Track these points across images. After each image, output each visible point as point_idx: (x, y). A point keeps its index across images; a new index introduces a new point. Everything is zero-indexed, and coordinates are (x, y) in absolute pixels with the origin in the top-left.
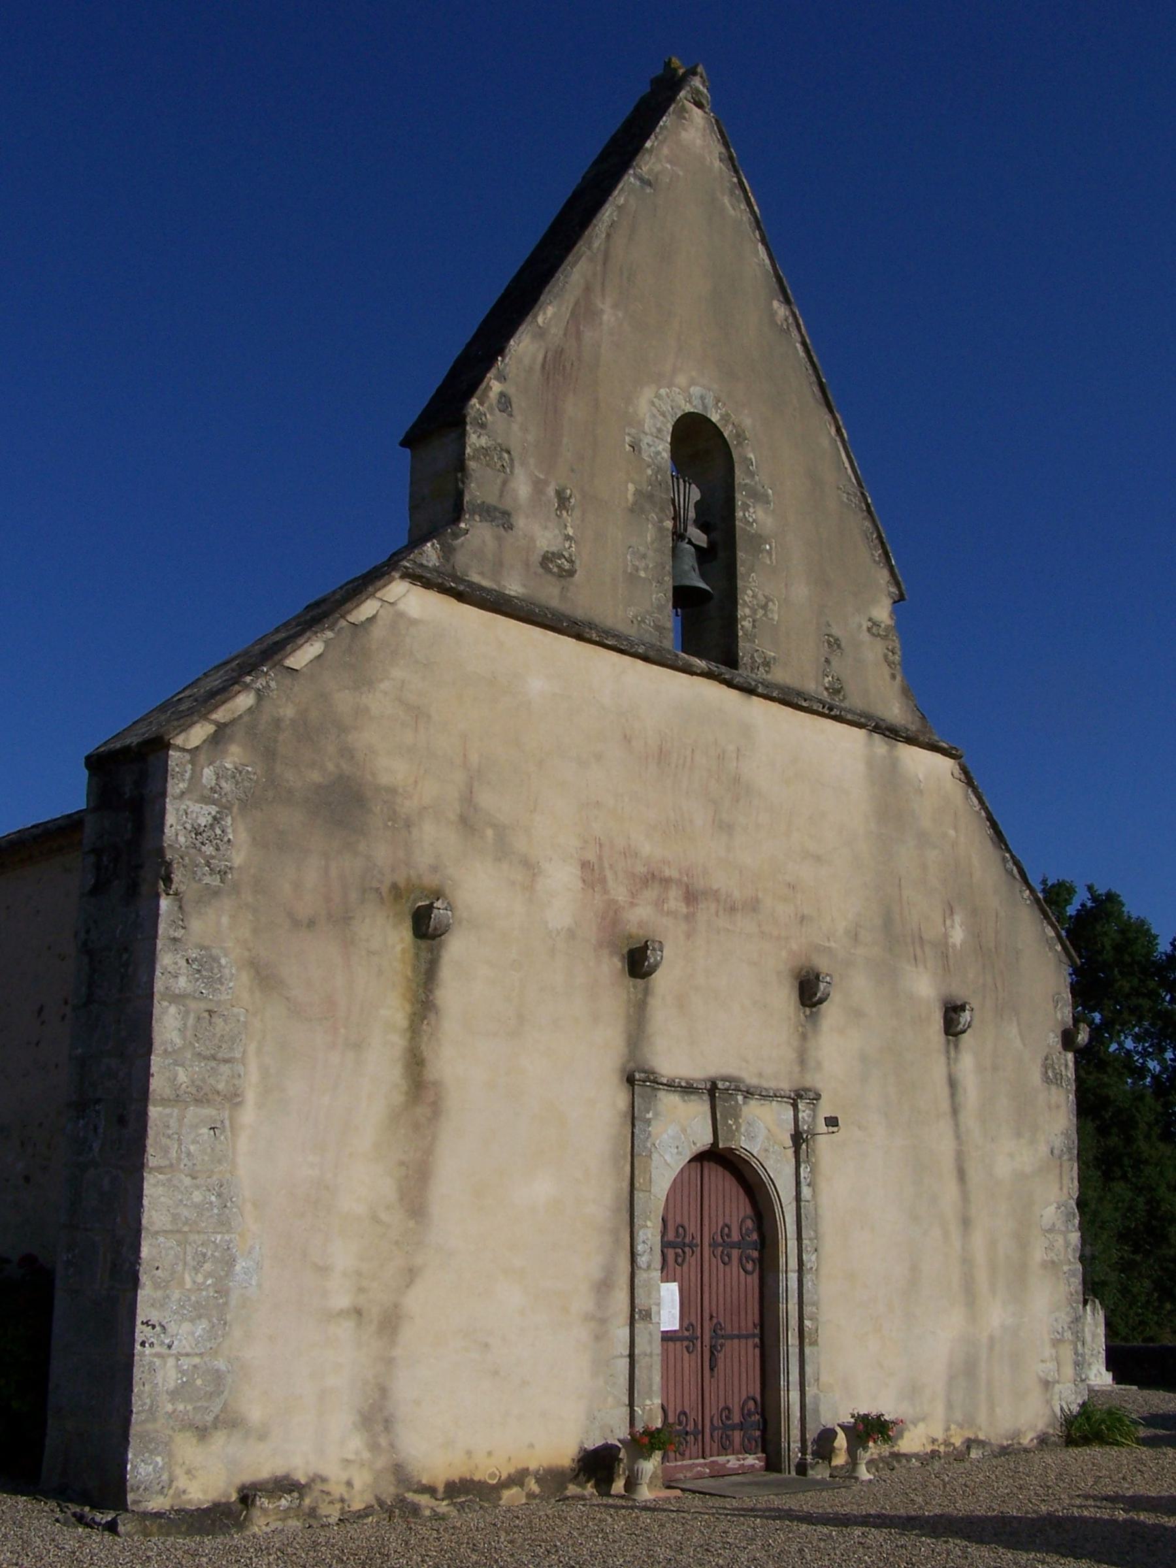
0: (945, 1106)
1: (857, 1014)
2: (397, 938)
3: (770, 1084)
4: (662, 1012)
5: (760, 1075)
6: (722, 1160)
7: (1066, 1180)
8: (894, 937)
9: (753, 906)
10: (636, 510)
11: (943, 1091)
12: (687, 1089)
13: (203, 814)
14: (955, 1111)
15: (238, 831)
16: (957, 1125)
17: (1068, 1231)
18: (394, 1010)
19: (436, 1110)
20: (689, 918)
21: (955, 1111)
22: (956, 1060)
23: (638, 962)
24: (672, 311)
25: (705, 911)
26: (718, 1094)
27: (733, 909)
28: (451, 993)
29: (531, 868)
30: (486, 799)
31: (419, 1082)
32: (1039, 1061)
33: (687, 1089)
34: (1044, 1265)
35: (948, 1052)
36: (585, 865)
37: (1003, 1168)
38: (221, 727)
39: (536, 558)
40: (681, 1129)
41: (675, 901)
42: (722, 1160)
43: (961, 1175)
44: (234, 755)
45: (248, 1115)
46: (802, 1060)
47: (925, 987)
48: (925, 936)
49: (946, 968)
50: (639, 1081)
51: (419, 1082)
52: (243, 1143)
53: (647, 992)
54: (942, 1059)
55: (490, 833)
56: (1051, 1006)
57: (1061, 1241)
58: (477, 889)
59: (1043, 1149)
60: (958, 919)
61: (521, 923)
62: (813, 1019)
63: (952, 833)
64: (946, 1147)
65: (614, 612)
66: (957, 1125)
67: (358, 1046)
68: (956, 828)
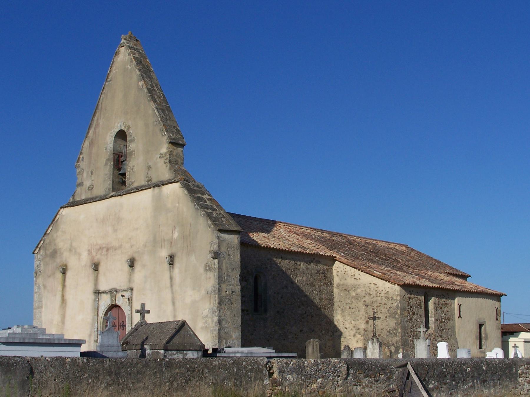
0: (168, 284)
1: (144, 266)
2: (59, 275)
3: (122, 288)
4: (101, 278)
5: (120, 286)
6: (114, 307)
7: (212, 301)
8: (156, 242)
9: (120, 247)
10: (106, 164)
11: (168, 281)
12: (106, 292)
13: (38, 263)
14: (172, 286)
15: (42, 264)
16: (172, 290)
17: (213, 317)
18: (60, 288)
19: (66, 304)
20: (107, 255)
21: (172, 286)
22: (173, 272)
23: (96, 267)
24: (124, 101)
25: (110, 251)
26: (113, 292)
27: (116, 249)
28: (68, 283)
29: (80, 254)
30: (74, 244)
31: (63, 300)
32: (203, 265)
33: (106, 292)
34: (202, 328)
35: (170, 269)
36: (89, 250)
37: (188, 300)
38: (40, 248)
39: (87, 188)
40: (105, 301)
41: (104, 252)
42: (114, 307)
43: (174, 303)
44: (42, 252)
45: (44, 309)
46: (130, 281)
47: (164, 253)
48: (165, 239)
49: (171, 246)
50: (97, 293)
51: (63, 300)
52: (43, 314)
53: (98, 274)
54: (168, 272)
55: (74, 250)
56: (209, 245)
57: (210, 320)
58: (73, 263)
59: (203, 292)
60: (176, 230)
61: (79, 266)
62: (133, 270)
63: (177, 205)
64: (169, 296)
65: (99, 191)
66: (172, 290)
67: (55, 295)
68: (179, 203)
